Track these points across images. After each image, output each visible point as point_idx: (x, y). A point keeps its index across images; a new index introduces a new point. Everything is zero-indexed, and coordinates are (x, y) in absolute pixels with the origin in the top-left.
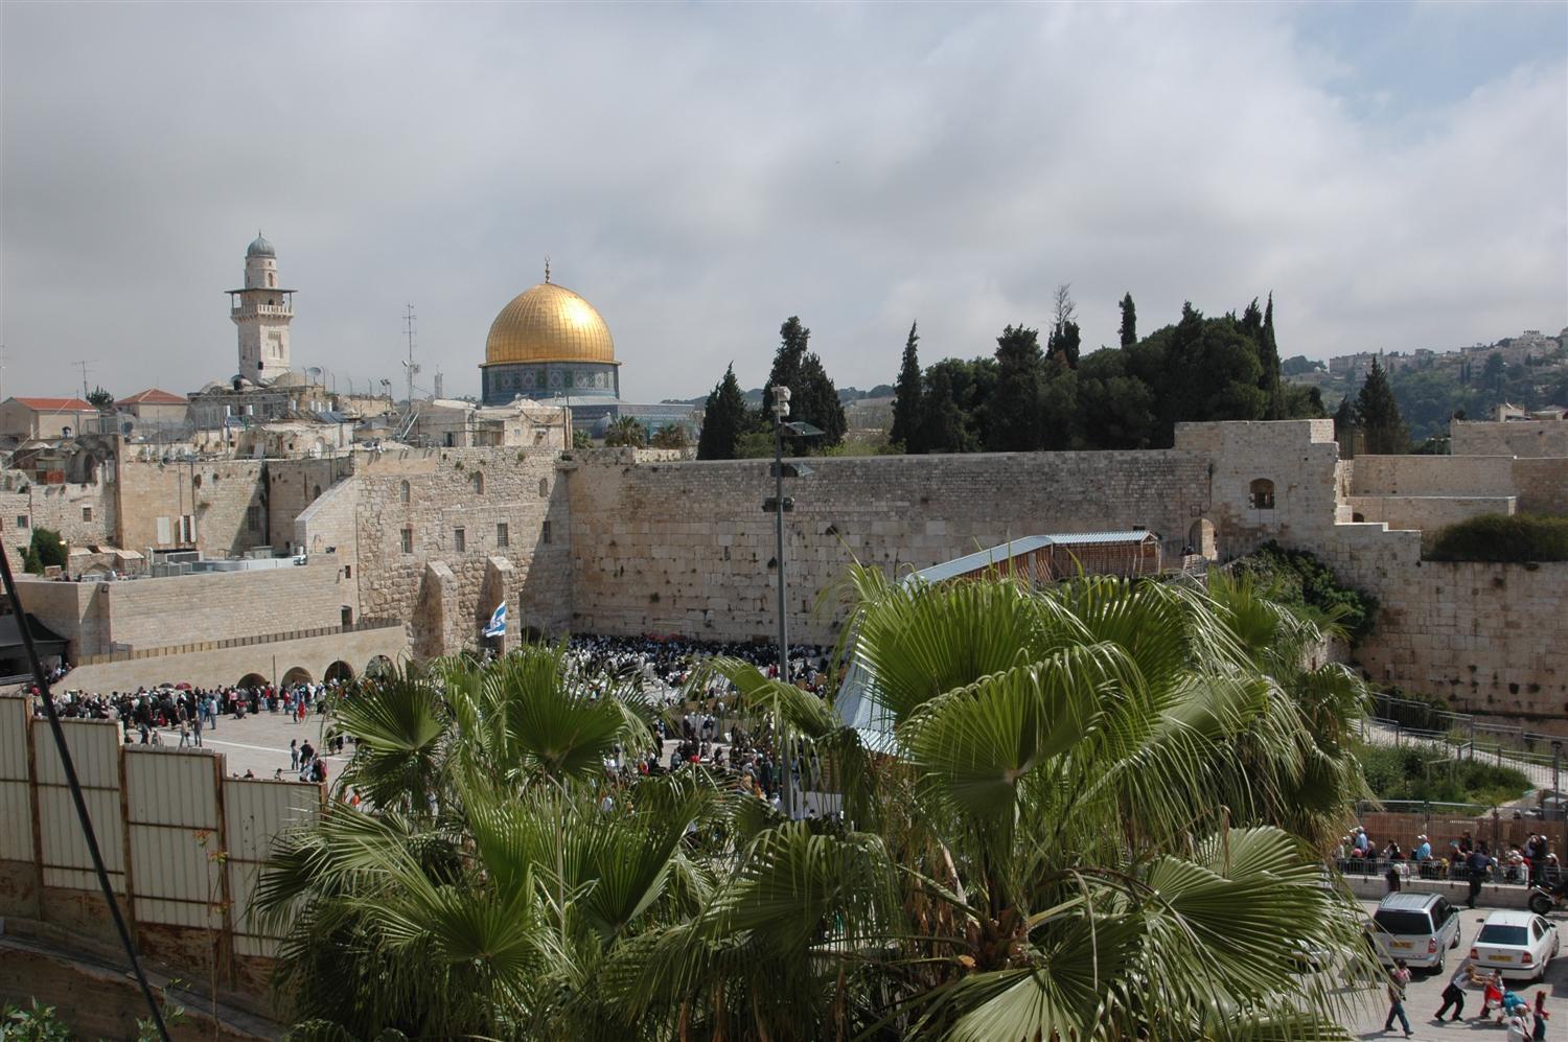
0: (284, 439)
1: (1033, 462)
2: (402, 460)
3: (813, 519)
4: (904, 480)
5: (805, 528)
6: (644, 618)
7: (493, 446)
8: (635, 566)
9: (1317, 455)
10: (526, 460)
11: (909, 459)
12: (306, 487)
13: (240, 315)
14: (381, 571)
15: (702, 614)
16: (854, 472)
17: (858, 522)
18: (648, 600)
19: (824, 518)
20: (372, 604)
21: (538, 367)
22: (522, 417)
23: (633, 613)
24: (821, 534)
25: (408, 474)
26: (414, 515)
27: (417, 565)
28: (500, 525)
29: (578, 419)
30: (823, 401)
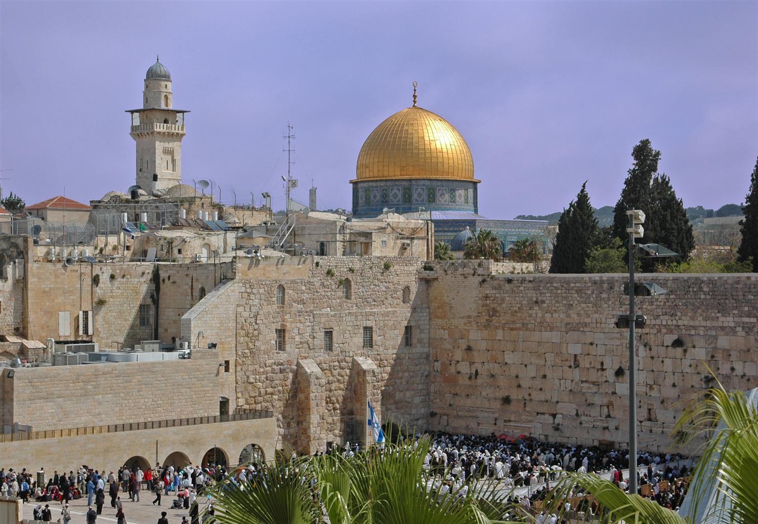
0: (174, 245)
2: (279, 266)
3: (659, 331)
4: (751, 297)
5: (651, 339)
6: (496, 419)
7: (362, 256)
8: (489, 370)
10: (392, 269)
13: (138, 132)
14: (257, 367)
15: (551, 418)
16: (700, 289)
17: (705, 335)
18: (501, 402)
19: (671, 332)
20: (247, 396)
22: (389, 230)
23: (486, 415)
24: (667, 346)
25: (285, 280)
26: (287, 317)
27: (289, 362)
28: (365, 328)
29: (440, 231)
30: (672, 219)
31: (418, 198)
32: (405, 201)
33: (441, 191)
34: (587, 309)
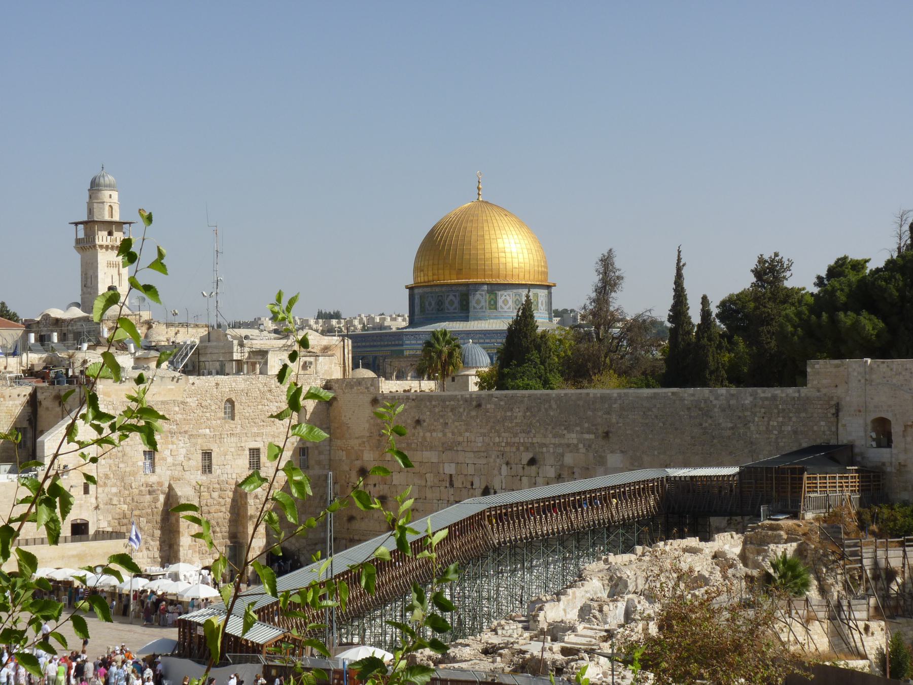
3: (518, 449)
4: (590, 413)
8: (379, 491)
11: (594, 394)
16: (550, 406)
17: (554, 453)
19: (527, 449)
21: (460, 288)
27: (160, 484)
28: (250, 449)
29: (359, 347)
31: (475, 305)
33: (503, 298)
34: (459, 427)
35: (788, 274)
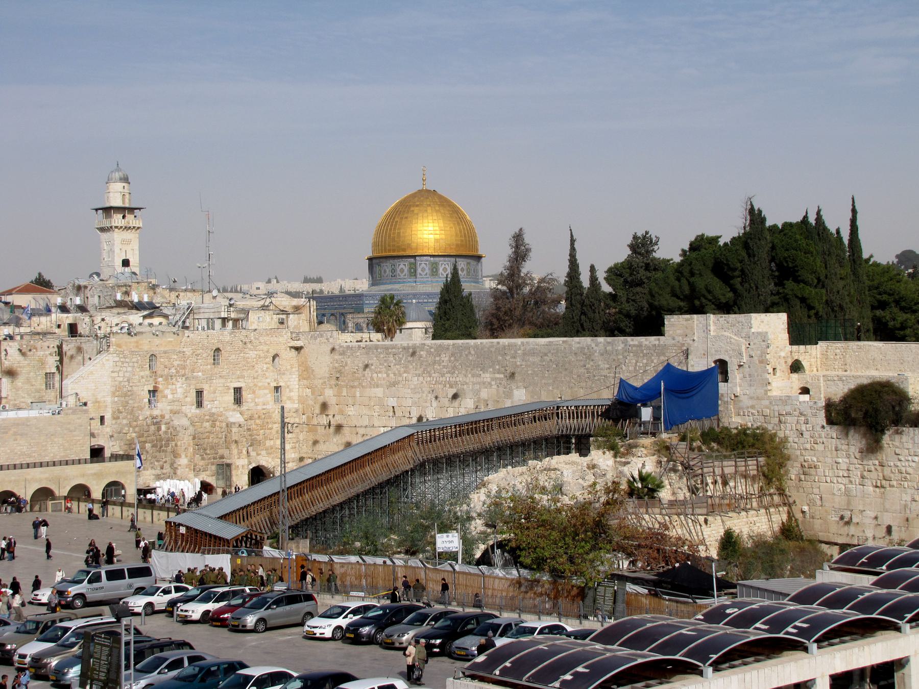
1: (578, 345)
9: (756, 341)
12: (84, 359)
16: (470, 353)
19: (451, 387)
22: (272, 307)
25: (155, 350)
27: (163, 416)
28: (234, 388)
32: (411, 276)
33: (443, 266)
35: (656, 248)
